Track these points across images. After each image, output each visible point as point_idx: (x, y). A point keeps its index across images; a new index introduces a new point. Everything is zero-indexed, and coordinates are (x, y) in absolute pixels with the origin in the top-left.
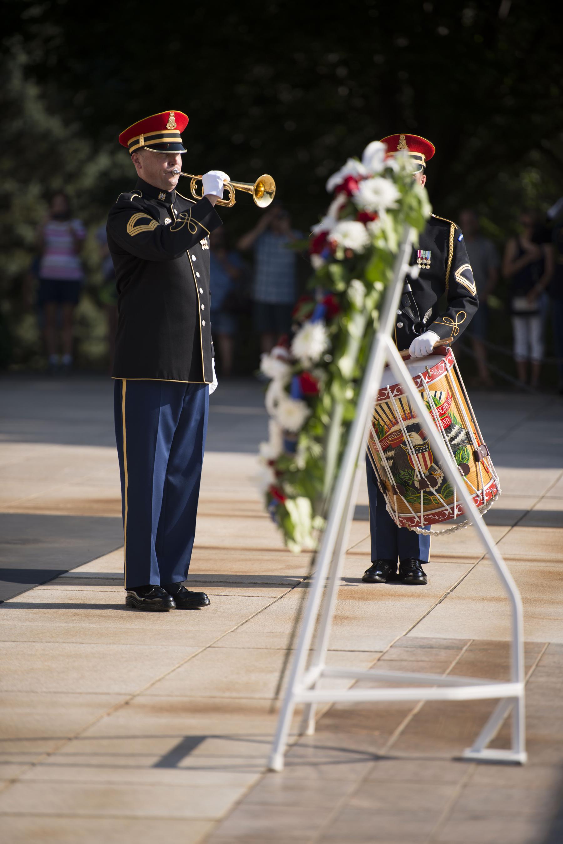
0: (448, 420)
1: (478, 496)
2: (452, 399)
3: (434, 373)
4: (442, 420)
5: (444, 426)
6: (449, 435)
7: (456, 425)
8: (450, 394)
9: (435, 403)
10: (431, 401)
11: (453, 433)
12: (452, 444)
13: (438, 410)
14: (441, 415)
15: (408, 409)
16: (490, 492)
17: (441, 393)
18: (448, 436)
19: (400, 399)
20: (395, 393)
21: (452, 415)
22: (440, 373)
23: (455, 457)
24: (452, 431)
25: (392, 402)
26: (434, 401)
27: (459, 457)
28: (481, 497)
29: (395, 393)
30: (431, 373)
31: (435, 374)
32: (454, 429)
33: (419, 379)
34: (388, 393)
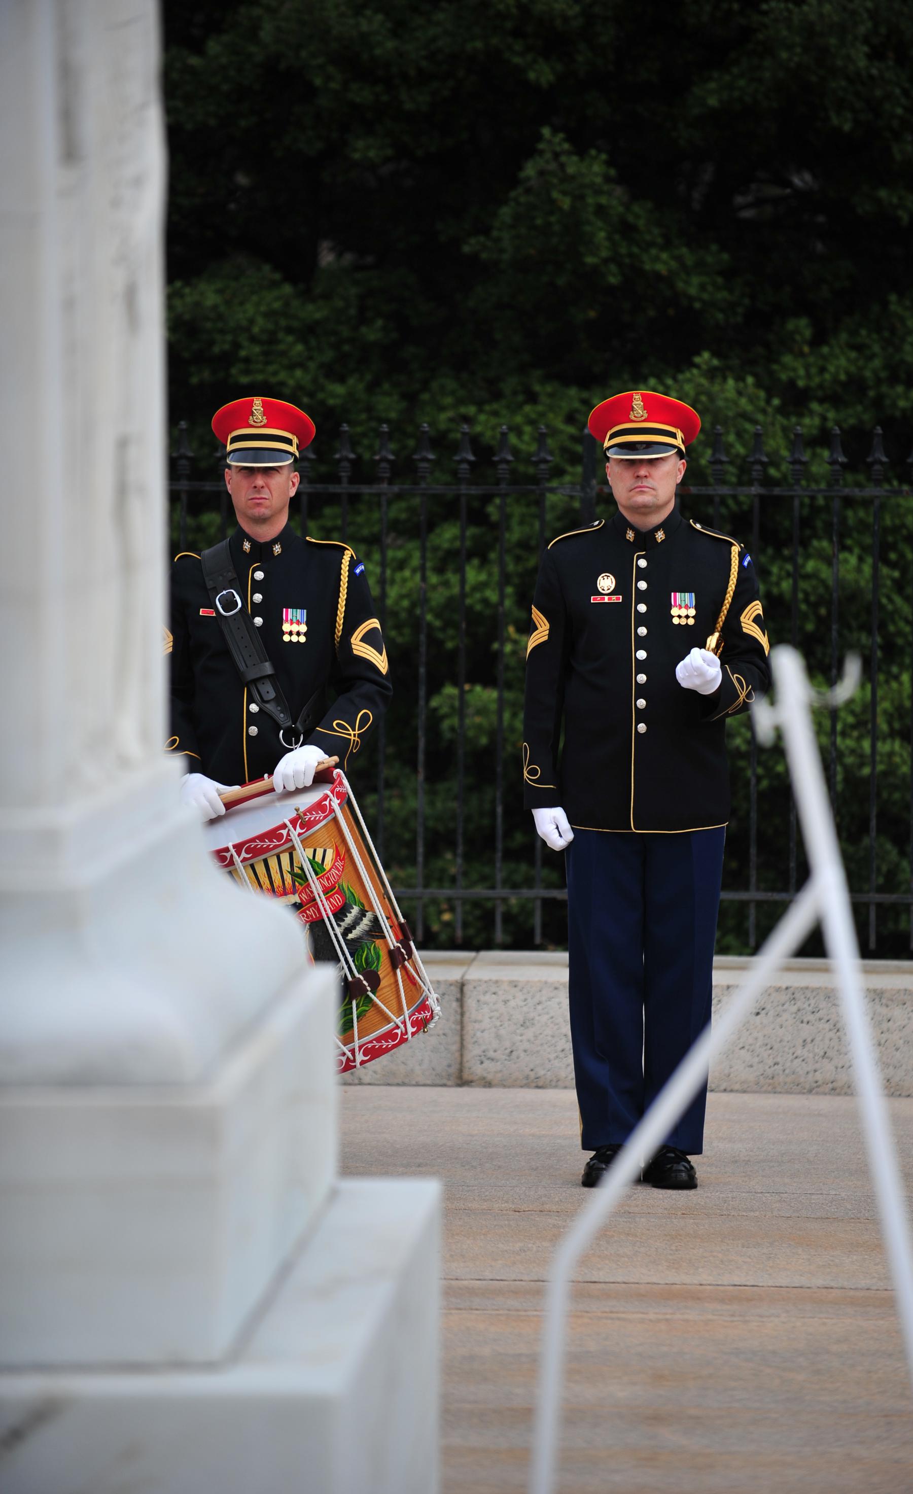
0: (338, 899)
1: (397, 1027)
2: (347, 860)
3: (310, 818)
4: (327, 899)
5: (333, 909)
6: (341, 923)
7: (354, 906)
8: (342, 851)
9: (314, 870)
10: (307, 867)
11: (349, 919)
12: (348, 940)
13: (320, 881)
14: (326, 891)
15: (267, 882)
16: (420, 1018)
17: (325, 851)
18: (339, 925)
19: (252, 866)
20: (244, 855)
21: (346, 889)
22: (321, 818)
23: (354, 961)
24: (347, 917)
25: (239, 870)
26: (312, 867)
27: (362, 961)
28: (404, 1029)
29: (244, 855)
30: (306, 818)
31: (312, 819)
32: (351, 913)
33: (285, 829)
34: (232, 856)
